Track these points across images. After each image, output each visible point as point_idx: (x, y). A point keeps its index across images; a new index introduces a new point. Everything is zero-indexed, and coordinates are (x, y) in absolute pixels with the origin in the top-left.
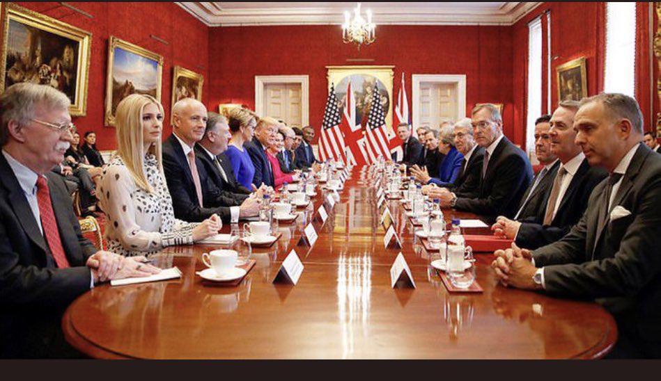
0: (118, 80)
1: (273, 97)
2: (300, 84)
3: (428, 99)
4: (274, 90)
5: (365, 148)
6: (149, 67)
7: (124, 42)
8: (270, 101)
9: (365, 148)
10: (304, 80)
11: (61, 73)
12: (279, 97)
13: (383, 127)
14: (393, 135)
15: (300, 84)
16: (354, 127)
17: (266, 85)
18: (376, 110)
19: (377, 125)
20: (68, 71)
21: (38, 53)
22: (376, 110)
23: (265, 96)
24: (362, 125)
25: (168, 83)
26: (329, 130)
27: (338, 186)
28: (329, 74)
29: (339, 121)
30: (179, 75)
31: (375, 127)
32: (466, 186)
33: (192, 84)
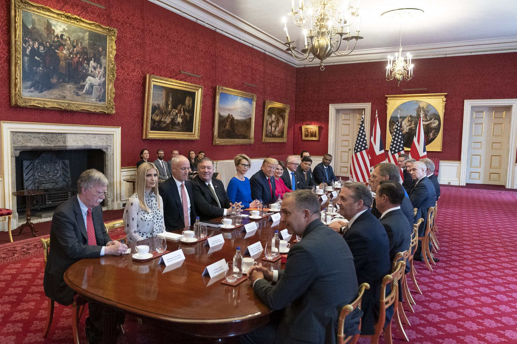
0: (222, 114)
2: (365, 109)
4: (344, 114)
6: (246, 104)
7: (226, 88)
8: (341, 122)
10: (367, 106)
11: (184, 113)
12: (349, 120)
15: (365, 109)
17: (338, 111)
20: (188, 112)
21: (170, 103)
23: (337, 119)
25: (261, 113)
28: (388, 101)
30: (270, 106)
33: (280, 112)
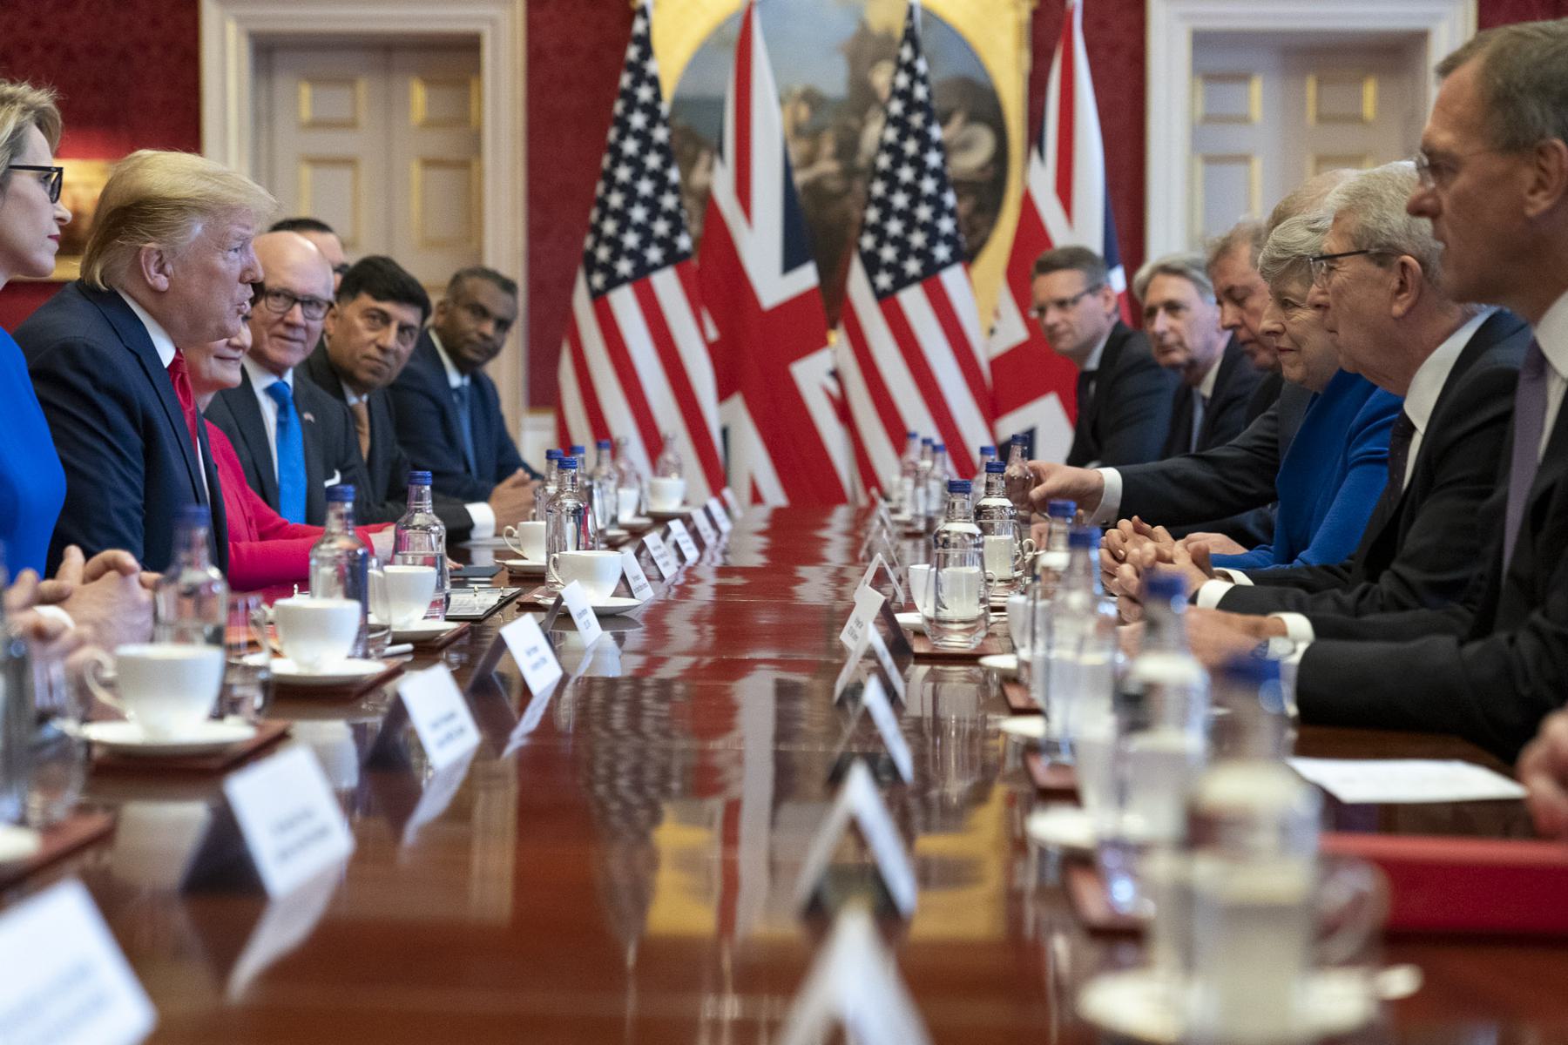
1: (316, 124)
3: (1232, 139)
4: (314, 80)
5: (844, 411)
8: (289, 142)
9: (844, 411)
12: (350, 125)
13: (953, 279)
14: (1014, 332)
16: (774, 282)
18: (906, 174)
19: (913, 266)
22: (906, 174)
23: (262, 118)
24: (822, 273)
26: (624, 302)
27: (612, 584)
29: (684, 242)
31: (902, 281)
32: (1413, 575)
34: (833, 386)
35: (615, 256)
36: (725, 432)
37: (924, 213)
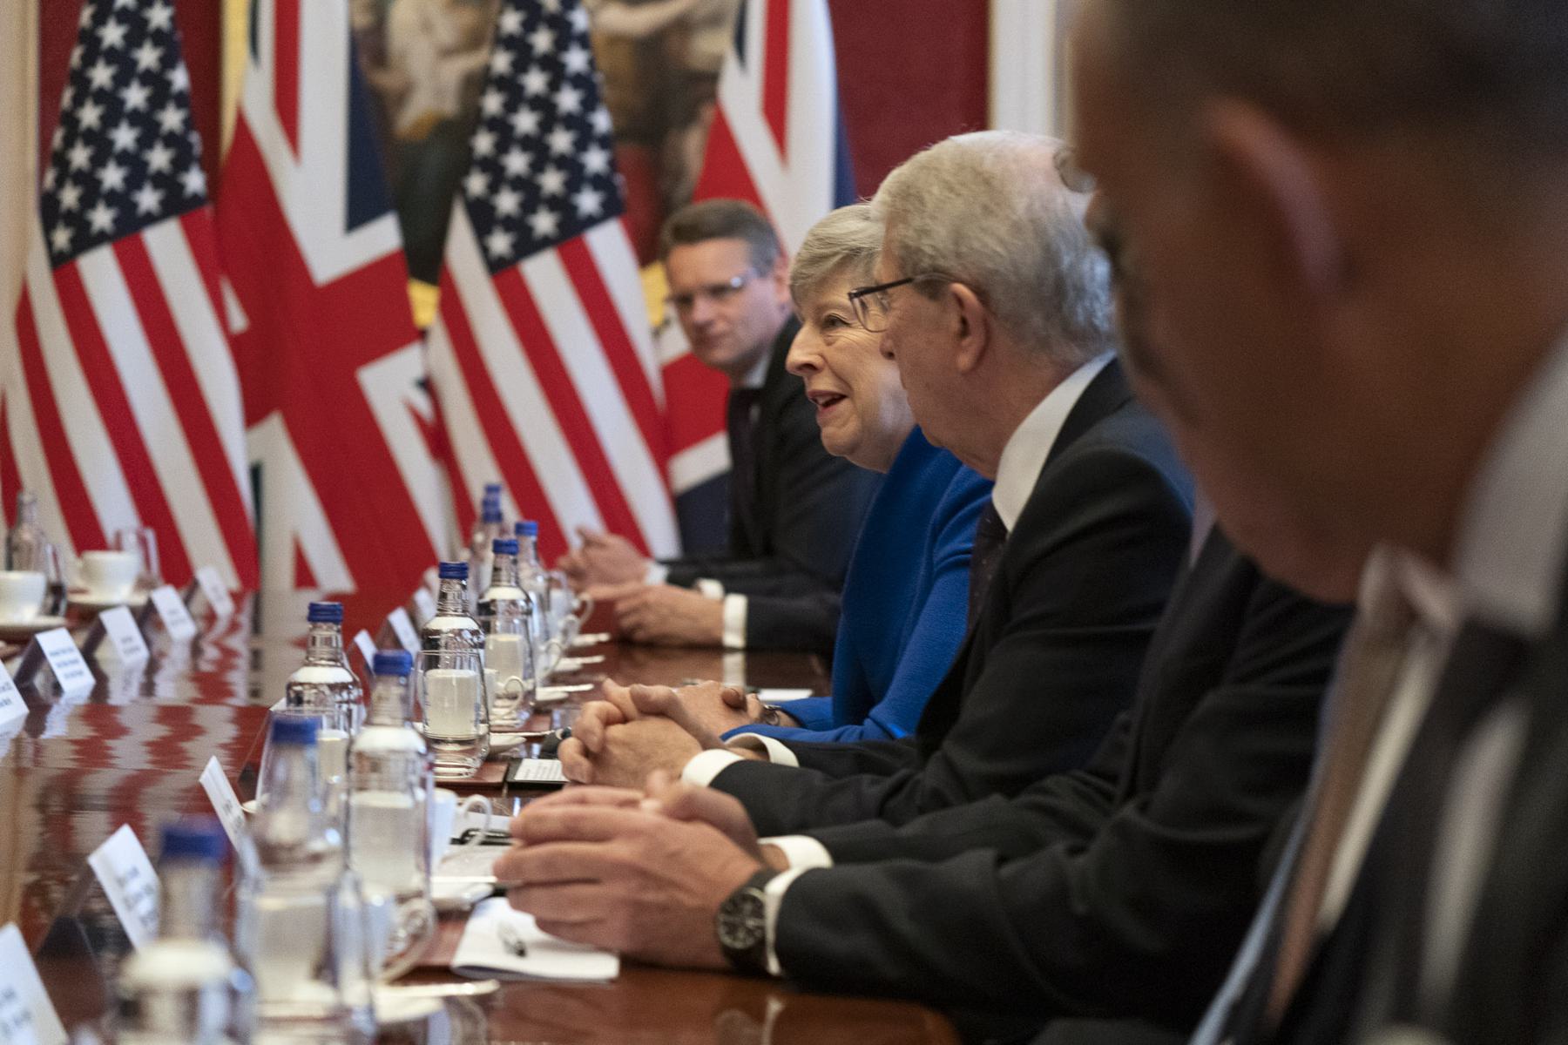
16: (333, 242)
18: (535, 82)
19: (544, 222)
24: (407, 228)
29: (195, 181)
31: (528, 245)
34: (422, 403)
35: (88, 202)
36: (256, 473)
37: (561, 141)
